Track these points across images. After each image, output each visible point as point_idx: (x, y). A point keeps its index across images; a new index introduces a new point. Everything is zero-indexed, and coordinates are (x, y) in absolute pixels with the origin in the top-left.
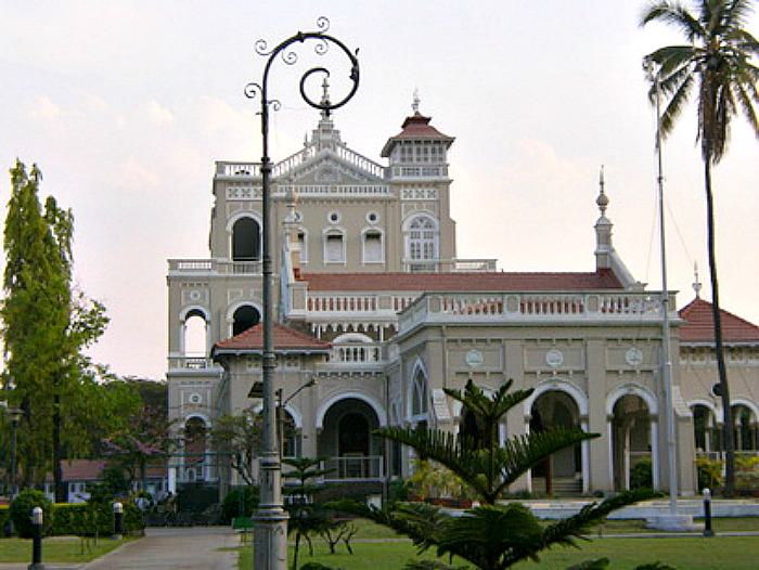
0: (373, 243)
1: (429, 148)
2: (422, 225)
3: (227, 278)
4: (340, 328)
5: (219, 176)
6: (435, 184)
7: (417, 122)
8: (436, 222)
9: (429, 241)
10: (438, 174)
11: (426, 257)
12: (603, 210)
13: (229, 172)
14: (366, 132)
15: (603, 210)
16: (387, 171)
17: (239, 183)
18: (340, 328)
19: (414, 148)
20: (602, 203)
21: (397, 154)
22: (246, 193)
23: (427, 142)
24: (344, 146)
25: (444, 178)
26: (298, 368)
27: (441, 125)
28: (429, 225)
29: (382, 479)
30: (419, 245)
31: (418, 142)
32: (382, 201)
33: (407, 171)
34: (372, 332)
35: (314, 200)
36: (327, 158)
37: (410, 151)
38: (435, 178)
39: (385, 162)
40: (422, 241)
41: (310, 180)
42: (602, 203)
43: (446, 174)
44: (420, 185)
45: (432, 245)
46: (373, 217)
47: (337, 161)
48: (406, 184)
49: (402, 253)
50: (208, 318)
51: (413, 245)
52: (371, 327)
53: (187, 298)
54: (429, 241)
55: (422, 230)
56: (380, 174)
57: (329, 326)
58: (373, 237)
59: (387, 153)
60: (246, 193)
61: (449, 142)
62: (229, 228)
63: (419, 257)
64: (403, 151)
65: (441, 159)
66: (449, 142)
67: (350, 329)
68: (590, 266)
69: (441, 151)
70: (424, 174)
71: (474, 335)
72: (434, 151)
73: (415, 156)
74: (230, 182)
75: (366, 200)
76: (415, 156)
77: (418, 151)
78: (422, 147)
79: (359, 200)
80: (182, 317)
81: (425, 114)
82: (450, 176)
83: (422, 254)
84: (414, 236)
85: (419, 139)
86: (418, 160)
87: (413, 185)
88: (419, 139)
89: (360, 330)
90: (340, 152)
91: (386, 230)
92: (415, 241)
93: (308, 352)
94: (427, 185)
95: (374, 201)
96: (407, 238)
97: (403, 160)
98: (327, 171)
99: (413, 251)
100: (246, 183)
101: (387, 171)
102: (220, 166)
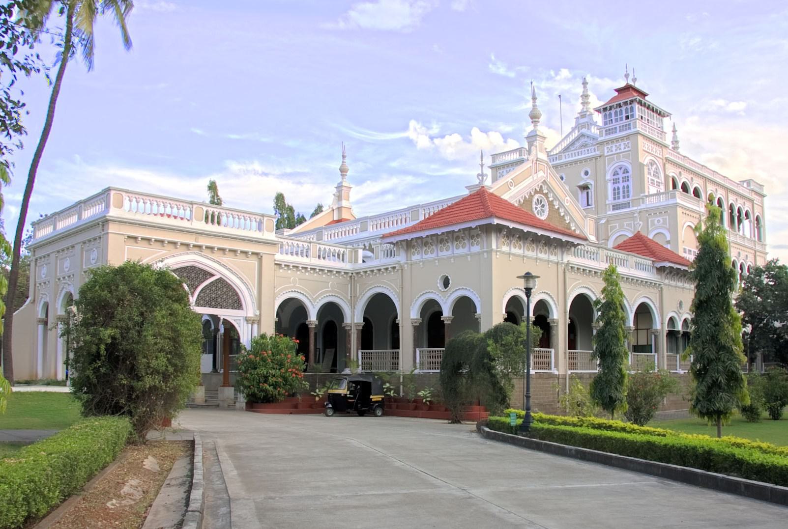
2: (621, 172)
6: (628, 137)
8: (629, 167)
9: (625, 184)
10: (630, 129)
11: (624, 197)
25: (633, 130)
30: (618, 188)
32: (591, 159)
37: (610, 115)
38: (628, 132)
40: (621, 186)
45: (628, 187)
46: (586, 173)
49: (606, 198)
51: (614, 189)
63: (619, 198)
70: (620, 131)
73: (613, 118)
75: (580, 161)
83: (621, 195)
86: (616, 120)
87: (612, 141)
91: (596, 181)
92: (616, 186)
95: (586, 160)
99: (614, 194)
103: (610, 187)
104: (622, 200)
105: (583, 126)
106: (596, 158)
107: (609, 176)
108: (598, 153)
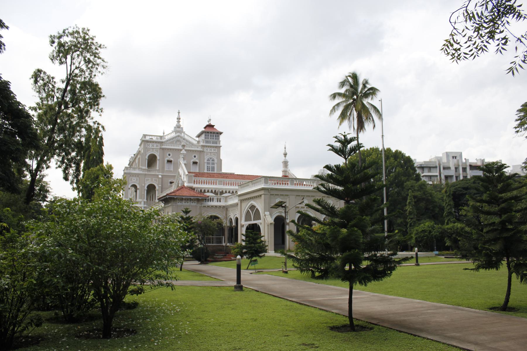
0: (195, 165)
1: (214, 135)
3: (145, 175)
4: (205, 191)
5: (144, 139)
6: (216, 147)
7: (210, 126)
9: (213, 166)
12: (285, 157)
13: (148, 138)
14: (193, 129)
15: (285, 157)
16: (198, 142)
17: (151, 142)
18: (205, 191)
19: (210, 135)
20: (285, 155)
21: (203, 136)
22: (153, 146)
23: (214, 133)
24: (184, 133)
25: (218, 145)
26: (195, 204)
27: (218, 128)
28: (213, 160)
29: (224, 244)
31: (211, 133)
32: (198, 151)
33: (207, 142)
34: (215, 193)
35: (176, 149)
36: (179, 136)
37: (208, 135)
39: (197, 139)
40: (211, 166)
41: (172, 143)
42: (285, 155)
43: (219, 143)
44: (211, 147)
47: (181, 137)
48: (206, 146)
50: (138, 187)
52: (215, 191)
53: (131, 180)
54: (213, 166)
55: (211, 162)
56: (195, 142)
57: (201, 190)
58: (195, 163)
59: (199, 136)
60: (153, 146)
61: (221, 133)
62: (147, 157)
64: (206, 135)
65: (218, 139)
66: (221, 133)
67: (208, 191)
68: (280, 174)
69: (218, 136)
71: (280, 193)
72: (216, 136)
73: (209, 137)
74: (147, 141)
75: (193, 151)
76: (209, 137)
77: (211, 136)
78: (212, 135)
79: (191, 151)
80: (129, 187)
81: (213, 124)
82: (221, 145)
84: (208, 163)
85: (211, 132)
87: (209, 146)
88: (211, 132)
89: (212, 192)
90: (183, 135)
91: (200, 161)
92: (209, 165)
93: (200, 198)
94: (213, 147)
95: (196, 151)
96: (206, 165)
97: (206, 138)
98: (178, 141)
100: (153, 142)
101: (198, 142)
102: (145, 136)
103: (206, 165)
104: (211, 172)
105: (178, 132)
106: (200, 151)
107: (206, 161)
108: (201, 150)
